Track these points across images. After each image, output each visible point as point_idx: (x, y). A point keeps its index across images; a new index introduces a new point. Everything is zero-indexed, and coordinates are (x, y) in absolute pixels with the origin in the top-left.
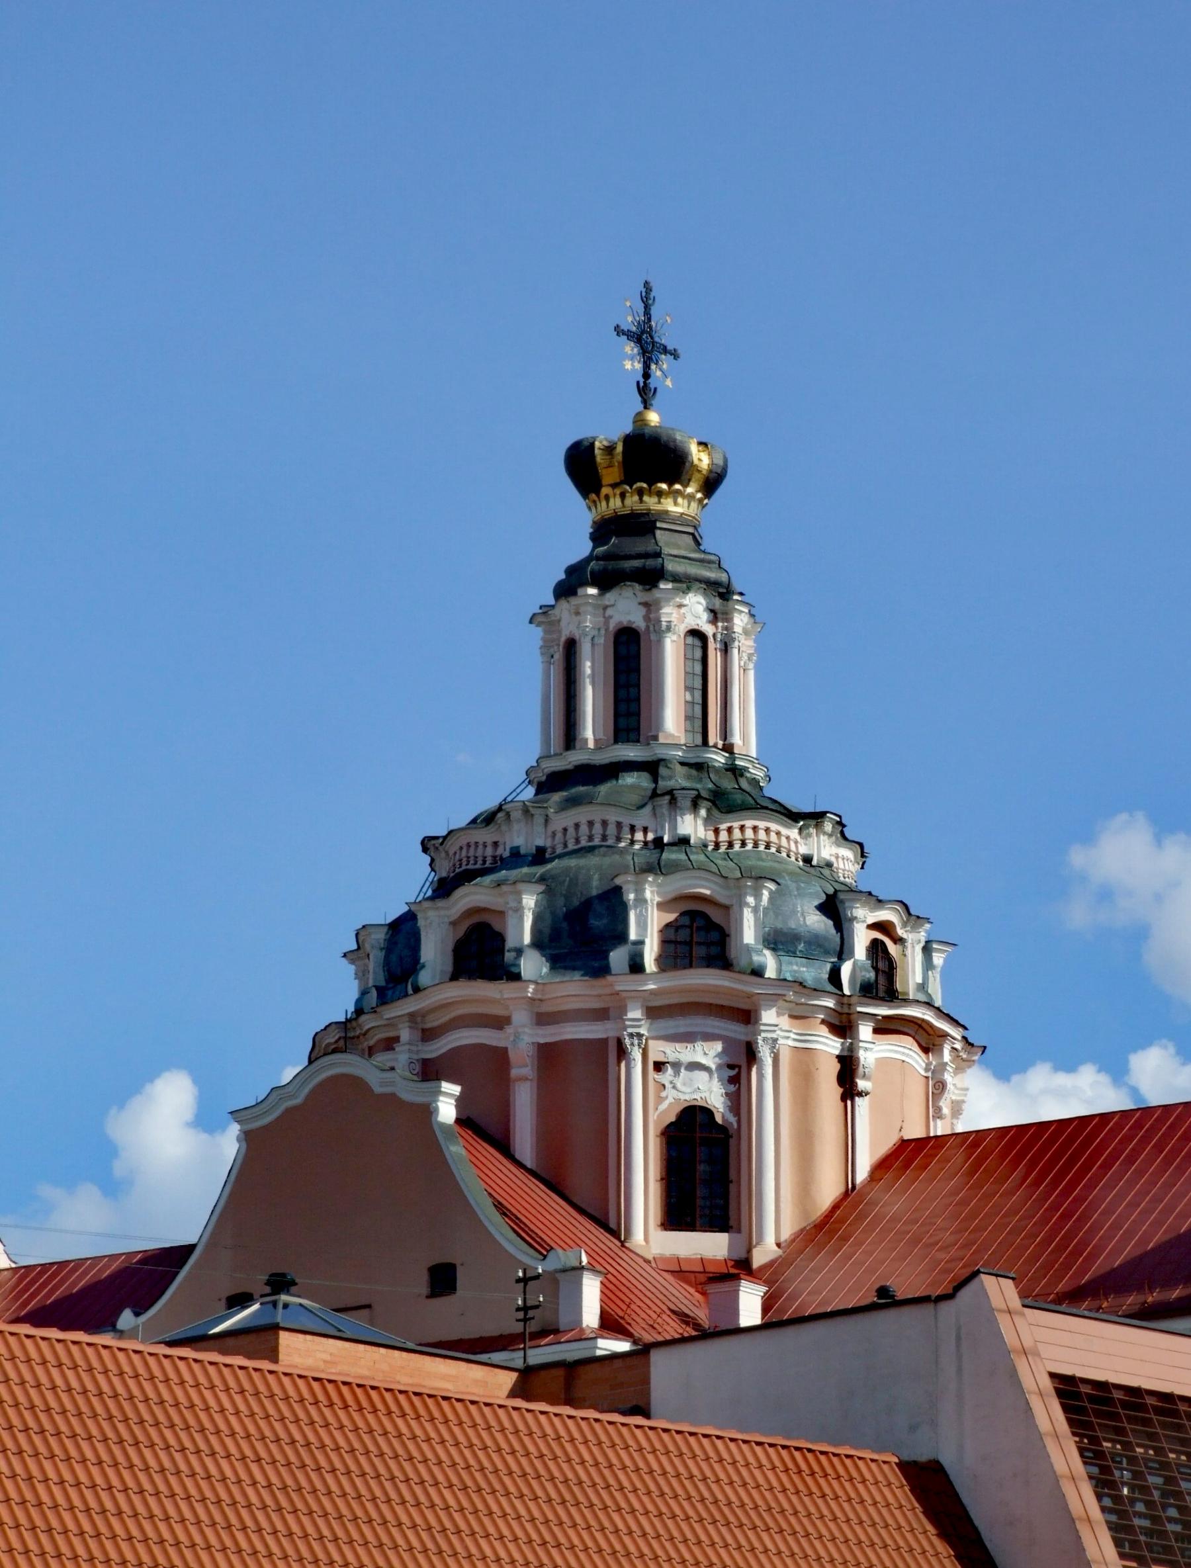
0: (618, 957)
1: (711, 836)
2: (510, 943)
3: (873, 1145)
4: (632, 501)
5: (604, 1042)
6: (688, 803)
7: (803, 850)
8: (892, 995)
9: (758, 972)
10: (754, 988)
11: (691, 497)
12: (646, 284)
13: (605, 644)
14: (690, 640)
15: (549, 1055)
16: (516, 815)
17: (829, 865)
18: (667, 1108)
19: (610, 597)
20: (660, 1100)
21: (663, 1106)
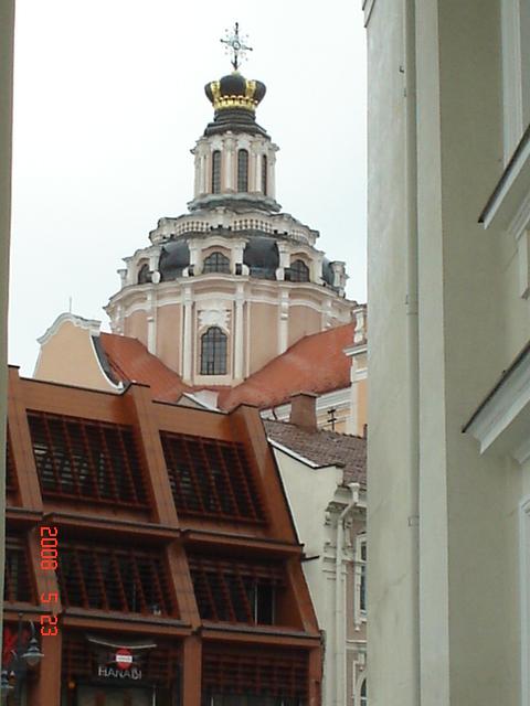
0: (185, 272)
1: (232, 225)
2: (151, 270)
3: (289, 337)
4: (224, 104)
5: (178, 304)
6: (222, 212)
7: (274, 228)
8: (309, 281)
9: (239, 272)
10: (232, 279)
13: (209, 157)
17: (286, 233)
18: (202, 329)
19: (210, 140)
21: (200, 328)
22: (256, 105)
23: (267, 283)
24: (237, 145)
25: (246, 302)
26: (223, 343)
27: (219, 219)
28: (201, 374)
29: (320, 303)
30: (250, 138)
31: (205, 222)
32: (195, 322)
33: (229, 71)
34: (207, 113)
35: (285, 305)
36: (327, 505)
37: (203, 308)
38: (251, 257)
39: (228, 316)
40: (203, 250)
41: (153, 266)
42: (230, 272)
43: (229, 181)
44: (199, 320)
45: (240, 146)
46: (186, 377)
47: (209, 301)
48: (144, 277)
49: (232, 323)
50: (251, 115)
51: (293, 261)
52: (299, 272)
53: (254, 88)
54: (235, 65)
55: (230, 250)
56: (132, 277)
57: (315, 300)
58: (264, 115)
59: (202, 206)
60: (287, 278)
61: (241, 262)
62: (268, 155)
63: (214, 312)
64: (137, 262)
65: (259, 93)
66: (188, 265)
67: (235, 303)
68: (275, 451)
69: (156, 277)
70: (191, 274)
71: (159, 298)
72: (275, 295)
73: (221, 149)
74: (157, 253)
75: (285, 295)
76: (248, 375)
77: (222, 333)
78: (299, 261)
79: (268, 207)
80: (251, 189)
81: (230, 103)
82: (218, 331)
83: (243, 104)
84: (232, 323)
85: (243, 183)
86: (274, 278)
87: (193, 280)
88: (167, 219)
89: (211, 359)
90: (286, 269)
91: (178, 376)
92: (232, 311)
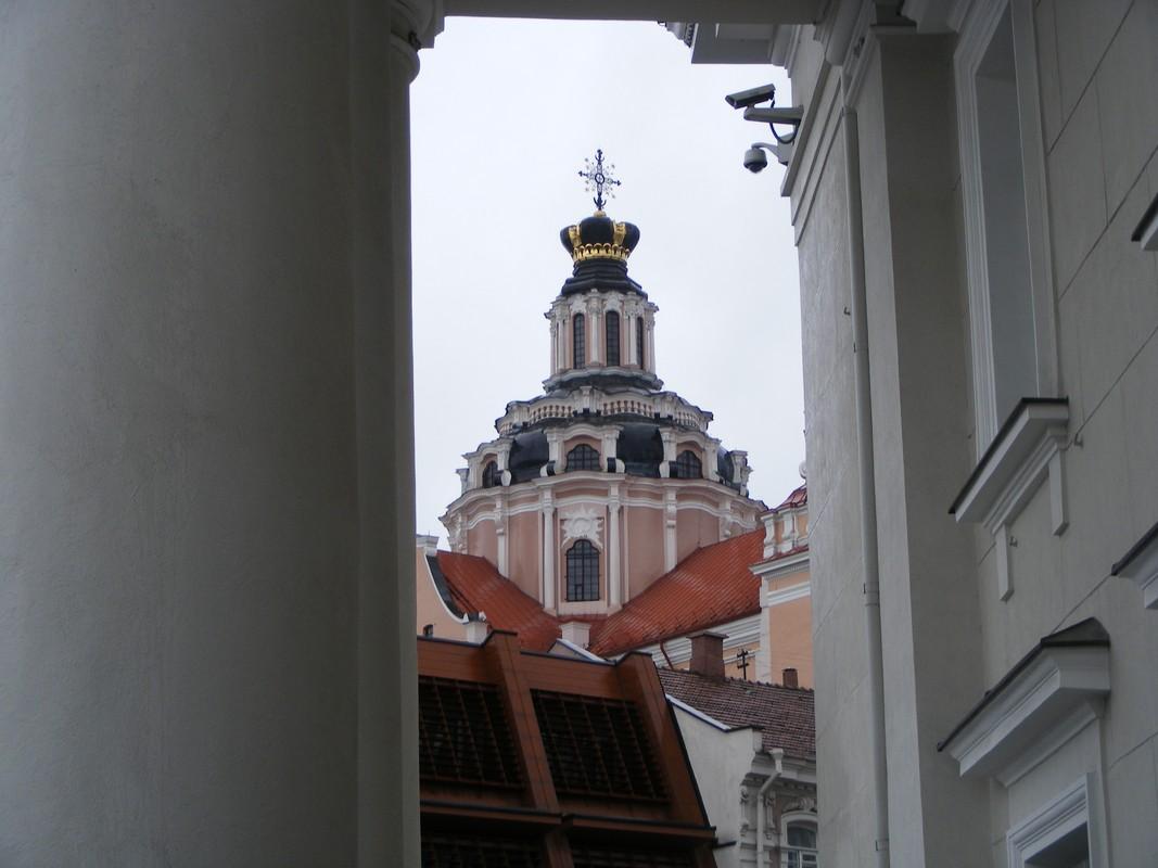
0: (544, 471)
1: (602, 408)
5: (536, 512)
8: (701, 477)
9: (612, 469)
10: (604, 477)
11: (615, 249)
12: (600, 152)
13: (569, 322)
14: (610, 316)
15: (511, 521)
16: (515, 407)
17: (670, 417)
19: (570, 300)
20: (562, 539)
21: (565, 542)
22: (628, 254)
23: (647, 482)
24: (604, 306)
25: (622, 507)
26: (594, 562)
27: (584, 402)
28: (568, 600)
29: (716, 505)
30: (621, 296)
31: (567, 406)
32: (558, 534)
33: (591, 211)
34: (564, 266)
35: (672, 509)
36: (742, 777)
37: (567, 515)
38: (626, 447)
39: (600, 526)
40: (566, 442)
41: (501, 464)
42: (600, 469)
43: (595, 352)
44: (563, 532)
45: (609, 307)
46: (549, 604)
47: (576, 507)
48: (490, 478)
49: (604, 535)
50: (621, 267)
51: (680, 452)
52: (689, 466)
53: (624, 232)
54: (599, 203)
55: (600, 441)
56: (475, 479)
57: (704, 499)
58: (638, 266)
59: (563, 385)
60: (674, 474)
61: (614, 455)
62: (643, 316)
63: (582, 521)
64: (482, 458)
65: (631, 237)
66: (545, 460)
67: (608, 507)
68: (676, 711)
69: (507, 477)
70: (551, 473)
71: (511, 504)
72: (659, 497)
73: (584, 311)
74: (506, 447)
75: (672, 496)
76: (627, 600)
77: (592, 547)
78: (687, 452)
79: (646, 383)
80: (625, 361)
81: (594, 252)
82: (588, 545)
83: (611, 253)
84: (604, 535)
85: (613, 353)
86: (657, 475)
87: (553, 481)
88: (518, 402)
89: (579, 581)
90: (671, 463)
91: (538, 604)
92: (604, 519)
